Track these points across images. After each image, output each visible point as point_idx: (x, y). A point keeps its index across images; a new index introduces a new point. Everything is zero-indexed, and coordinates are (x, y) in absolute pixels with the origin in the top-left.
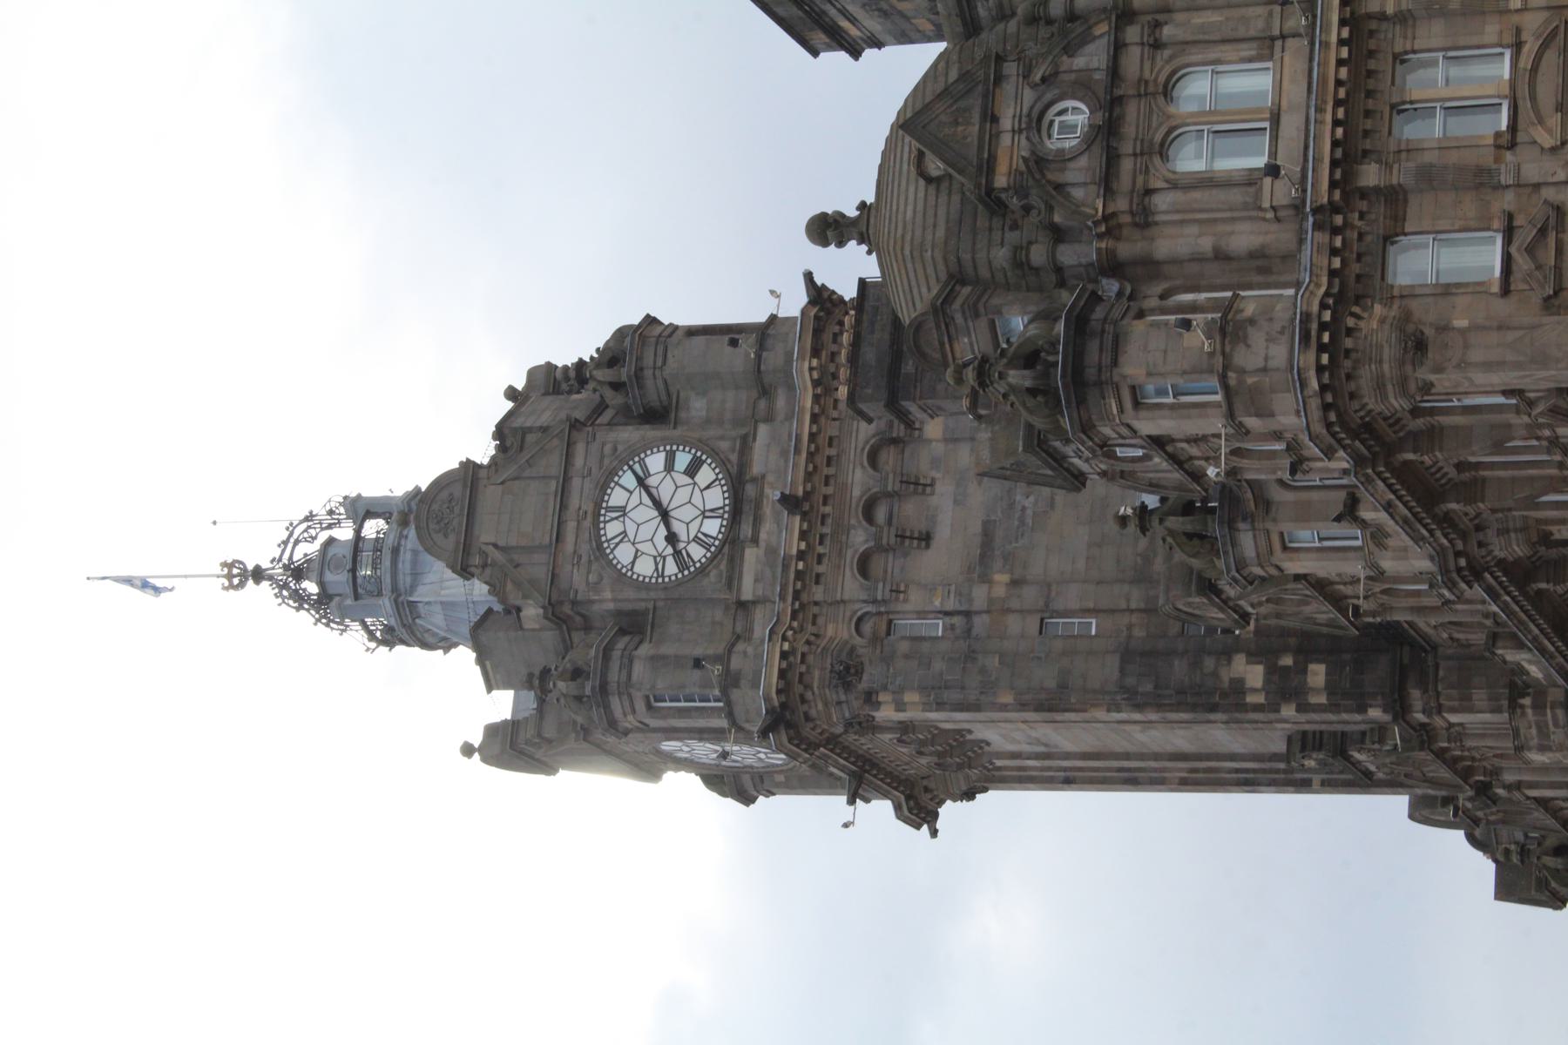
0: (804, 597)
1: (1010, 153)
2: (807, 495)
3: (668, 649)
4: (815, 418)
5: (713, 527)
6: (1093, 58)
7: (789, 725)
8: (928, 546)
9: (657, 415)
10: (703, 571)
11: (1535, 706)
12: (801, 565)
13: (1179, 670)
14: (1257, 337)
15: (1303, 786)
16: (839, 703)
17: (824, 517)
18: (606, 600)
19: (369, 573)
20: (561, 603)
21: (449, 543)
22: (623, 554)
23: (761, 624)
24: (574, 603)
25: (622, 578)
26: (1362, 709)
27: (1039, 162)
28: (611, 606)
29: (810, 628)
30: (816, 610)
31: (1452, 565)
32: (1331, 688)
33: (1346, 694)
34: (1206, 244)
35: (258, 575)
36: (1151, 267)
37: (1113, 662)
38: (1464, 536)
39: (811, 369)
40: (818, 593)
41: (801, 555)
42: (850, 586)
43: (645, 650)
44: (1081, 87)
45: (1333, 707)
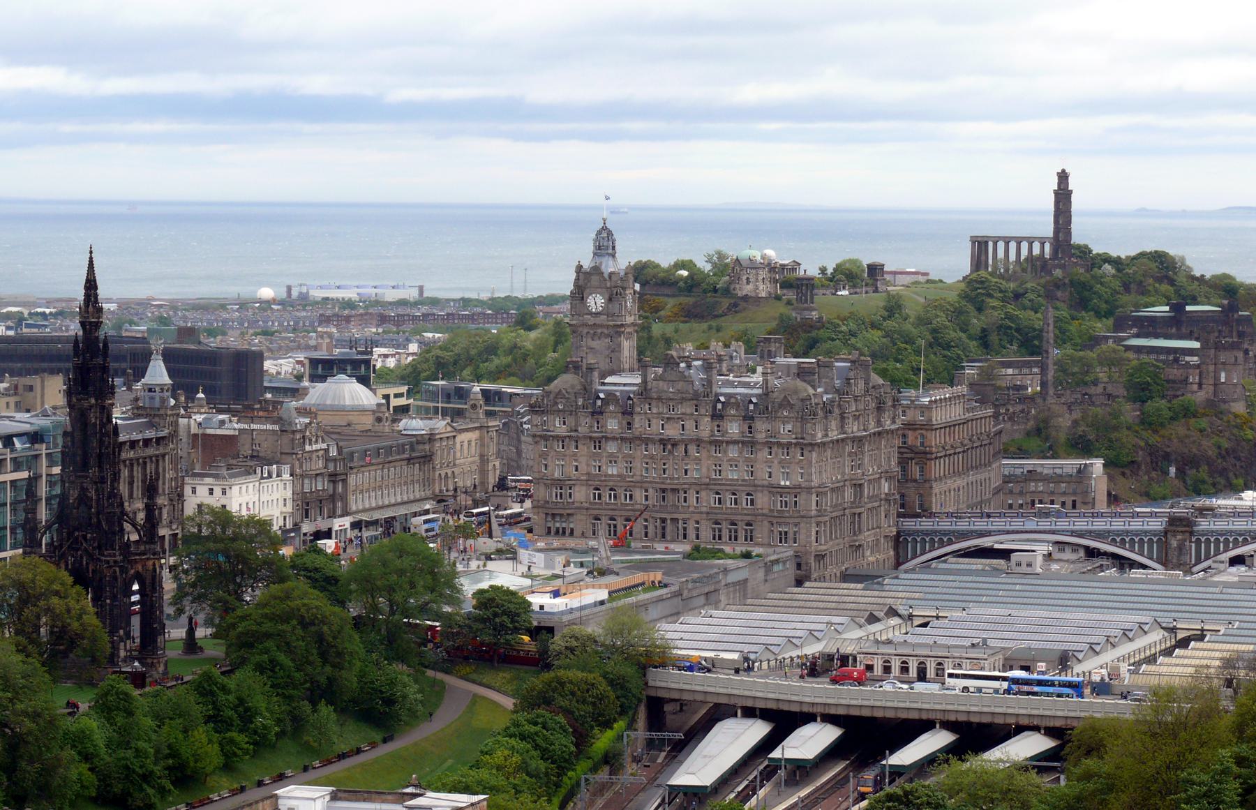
9: (610, 300)
42: (585, 331)
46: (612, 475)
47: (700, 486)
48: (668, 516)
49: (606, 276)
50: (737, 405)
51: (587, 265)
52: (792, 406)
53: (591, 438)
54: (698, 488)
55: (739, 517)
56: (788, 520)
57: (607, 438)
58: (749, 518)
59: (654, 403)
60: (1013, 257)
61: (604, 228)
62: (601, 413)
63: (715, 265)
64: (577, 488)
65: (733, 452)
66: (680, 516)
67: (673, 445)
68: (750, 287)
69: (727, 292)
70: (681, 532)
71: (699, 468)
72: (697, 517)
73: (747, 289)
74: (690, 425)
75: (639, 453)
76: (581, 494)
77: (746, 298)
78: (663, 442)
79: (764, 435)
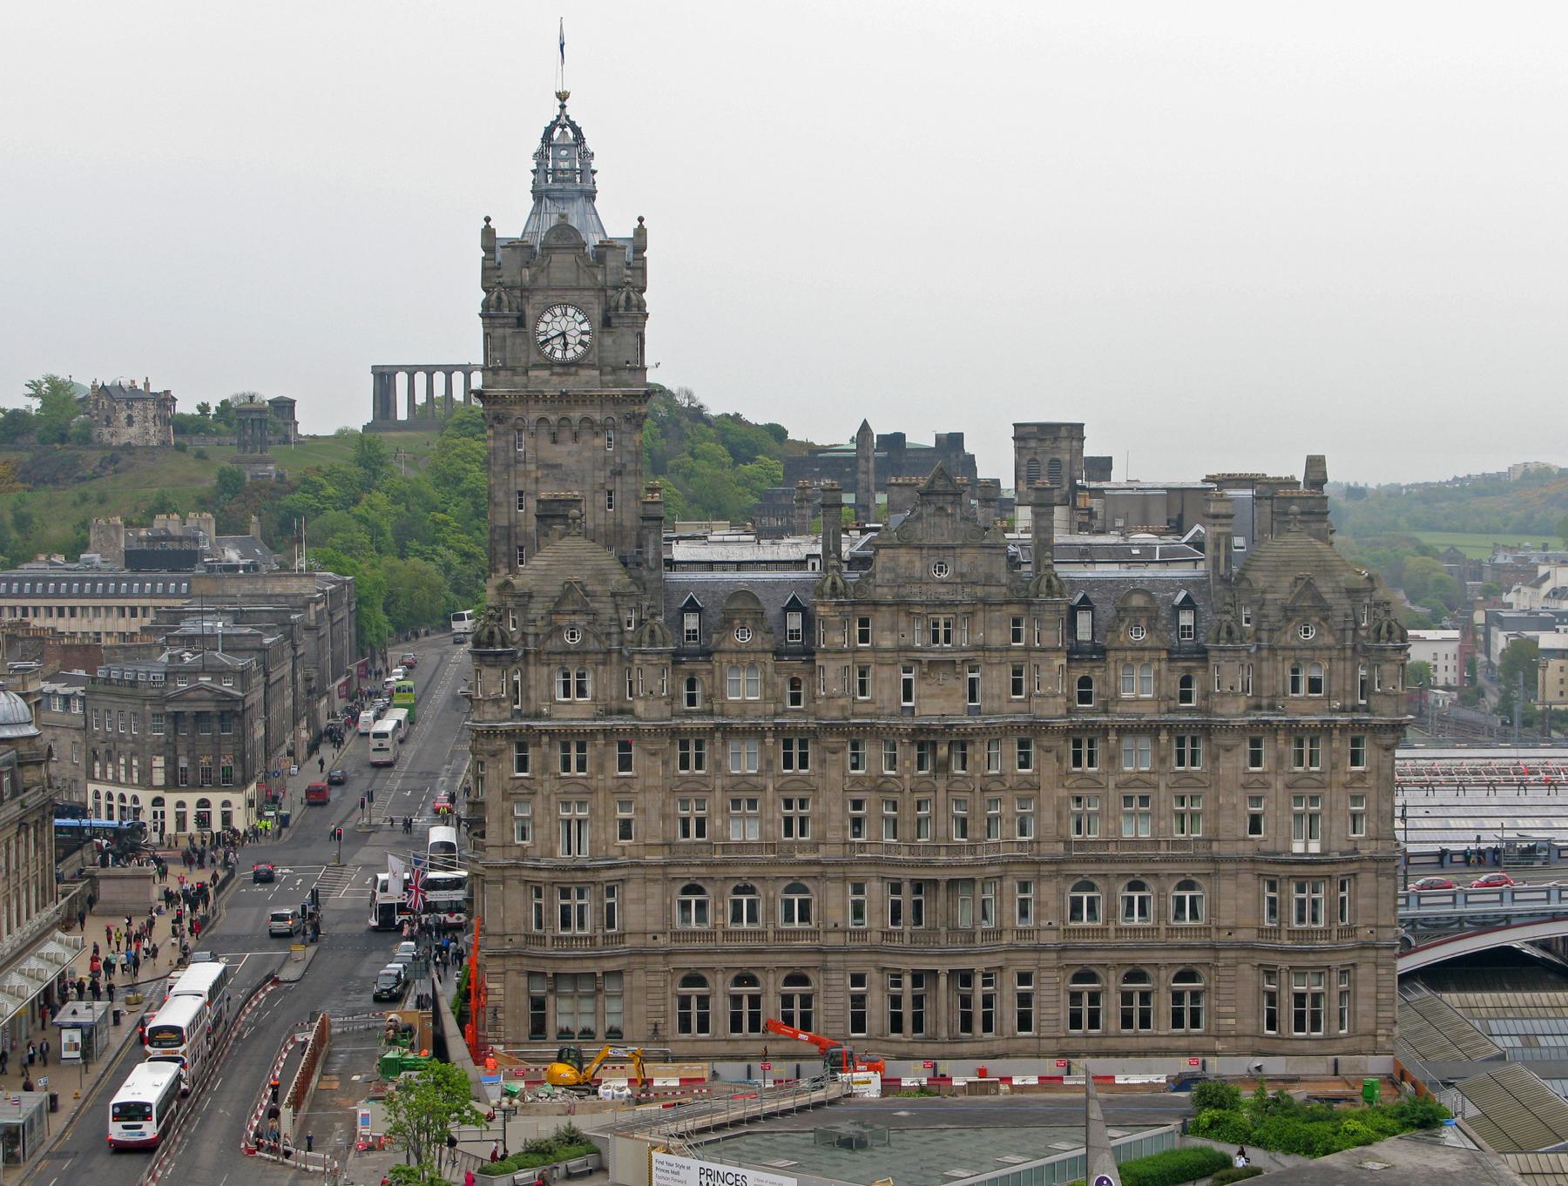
1: (564, 621)
3: (509, 343)
5: (558, 354)
6: (593, 645)
9: (607, 323)
10: (540, 353)
13: (503, 548)
14: (495, 709)
18: (530, 312)
19: (563, 166)
21: (552, 242)
22: (547, 317)
23: (519, 379)
25: (539, 319)
27: (560, 629)
34: (532, 683)
35: (563, 107)
36: (527, 663)
37: (505, 523)
42: (534, 416)
43: (509, 331)
44: (584, 641)
46: (743, 846)
47: (1032, 868)
48: (943, 966)
49: (589, 249)
50: (1150, 616)
51: (511, 227)
52: (1324, 611)
53: (674, 732)
54: (1026, 873)
55: (1159, 957)
56: (1326, 960)
57: (728, 732)
58: (1190, 957)
59: (880, 620)
60: (421, 398)
61: (563, 120)
62: (707, 654)
63: (44, 398)
64: (632, 891)
65: (1138, 759)
66: (978, 964)
67: (951, 744)
68: (135, 430)
69: (86, 439)
70: (978, 1011)
71: (1045, 808)
72: (1026, 963)
73: (129, 435)
74: (994, 681)
75: (834, 773)
76: (643, 909)
77: (128, 447)
78: (924, 740)
79: (1242, 703)
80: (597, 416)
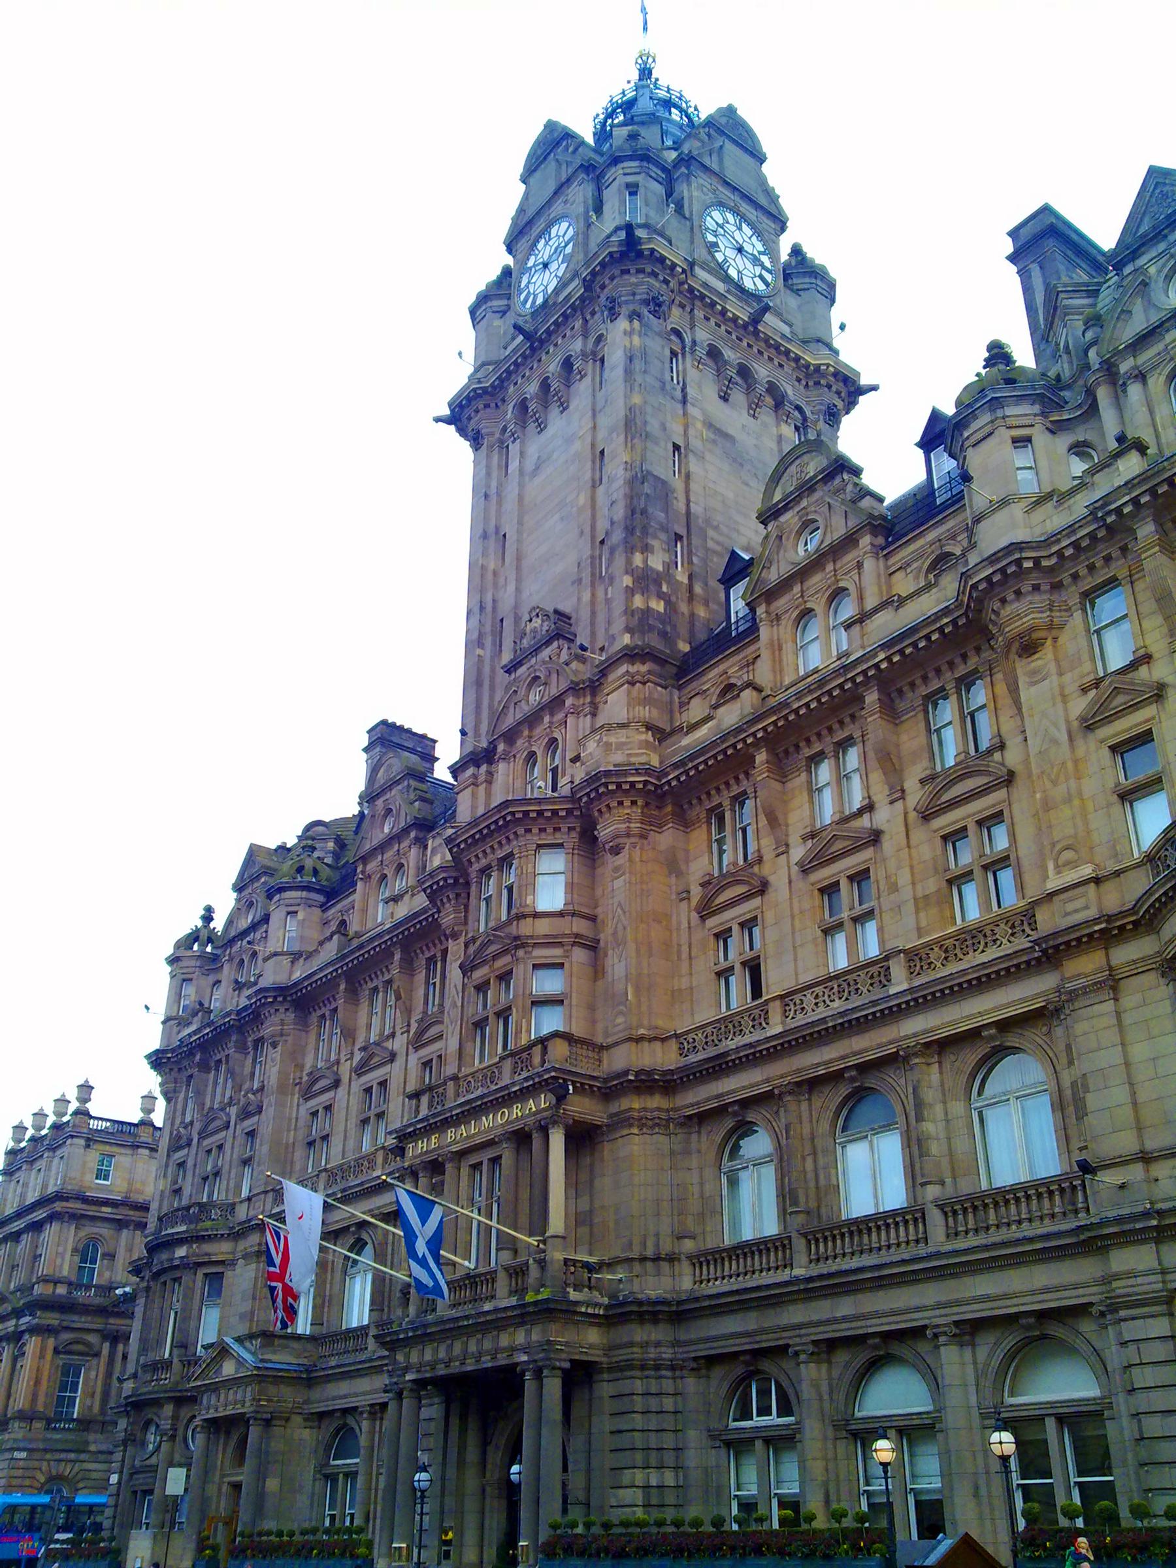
0: (698, 303)
2: (756, 333)
4: (797, 359)
5: (733, 273)
7: (623, 255)
8: (720, 397)
11: (647, 742)
12: (719, 308)
15: (474, 643)
16: (634, 294)
17: (740, 340)
20: (688, 168)
22: (716, 215)
24: (688, 176)
26: (628, 629)
28: (686, 194)
29: (678, 299)
30: (688, 309)
31: (1024, 555)
32: (647, 612)
33: (641, 622)
38: (1051, 570)
39: (828, 365)
40: (699, 314)
41: (724, 312)
42: (703, 335)
45: (629, 612)
80: (790, 390)
